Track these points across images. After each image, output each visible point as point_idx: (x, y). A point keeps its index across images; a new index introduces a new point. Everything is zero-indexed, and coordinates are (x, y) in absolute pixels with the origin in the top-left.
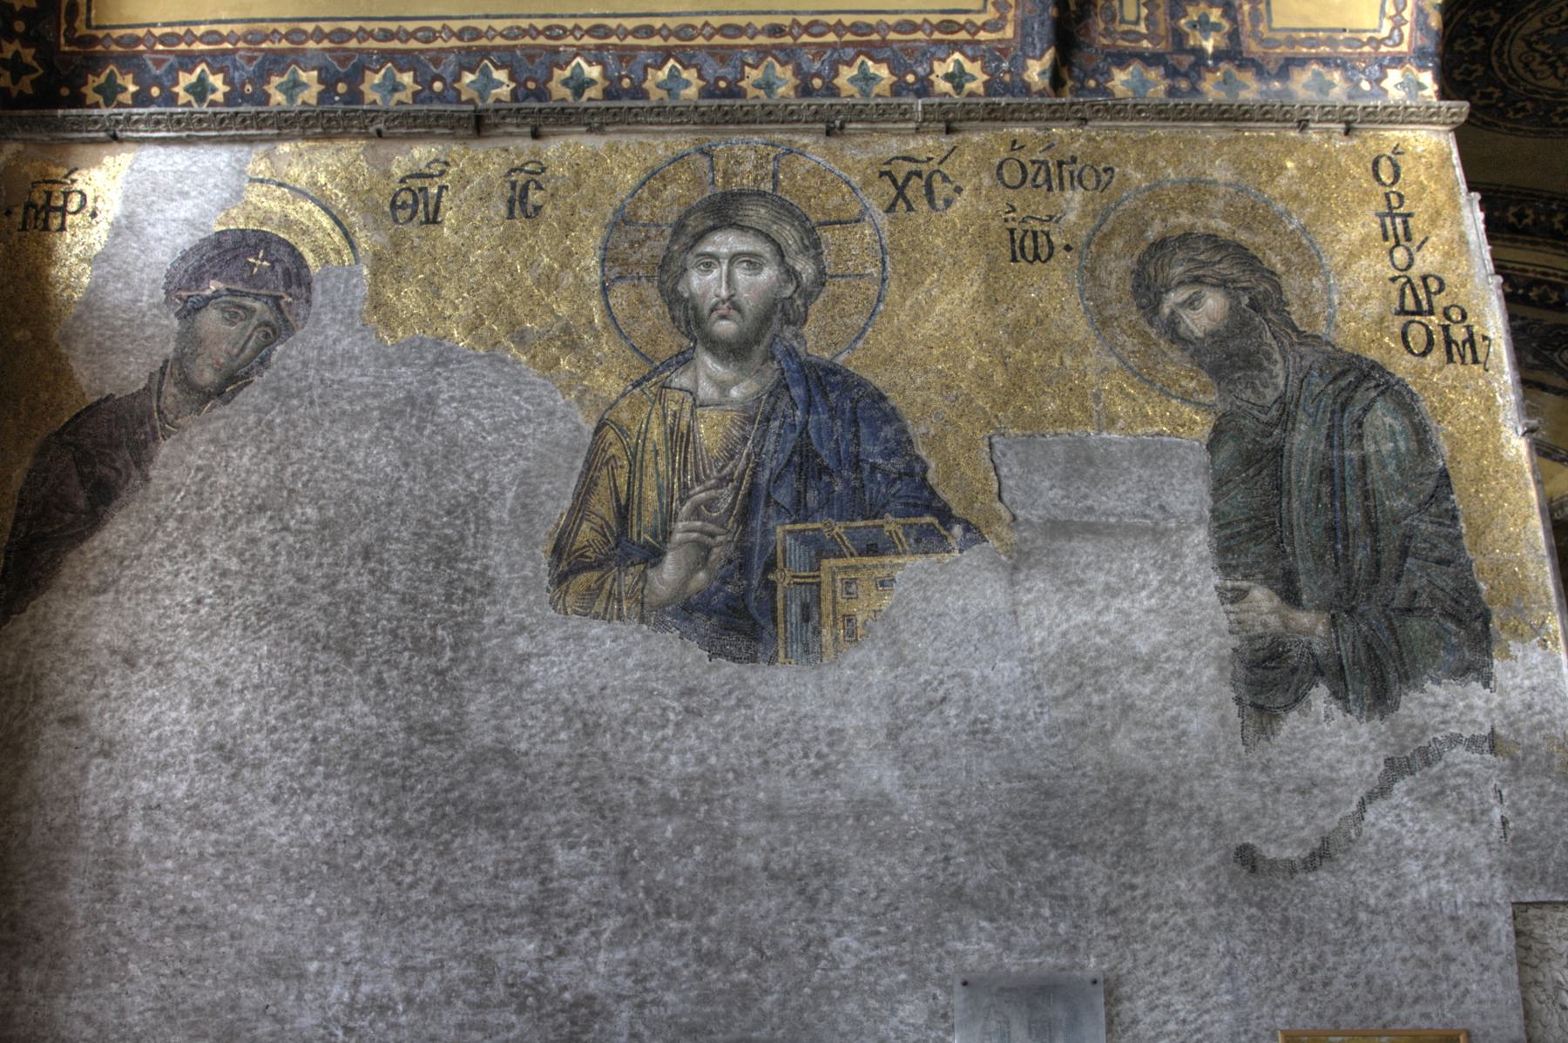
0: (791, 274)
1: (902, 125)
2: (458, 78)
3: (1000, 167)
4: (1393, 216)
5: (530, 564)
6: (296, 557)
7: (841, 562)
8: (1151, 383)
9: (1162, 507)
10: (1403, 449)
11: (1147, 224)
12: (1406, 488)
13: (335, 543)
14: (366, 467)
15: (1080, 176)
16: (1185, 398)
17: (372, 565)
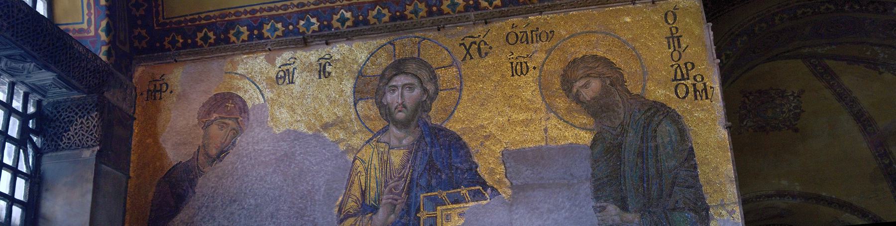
0: (425, 90)
1: (468, 23)
2: (298, 23)
3: (508, 35)
5: (330, 216)
6: (247, 219)
7: (444, 207)
8: (567, 122)
10: (674, 140)
13: (261, 212)
14: (271, 182)
16: (583, 128)
17: (274, 220)
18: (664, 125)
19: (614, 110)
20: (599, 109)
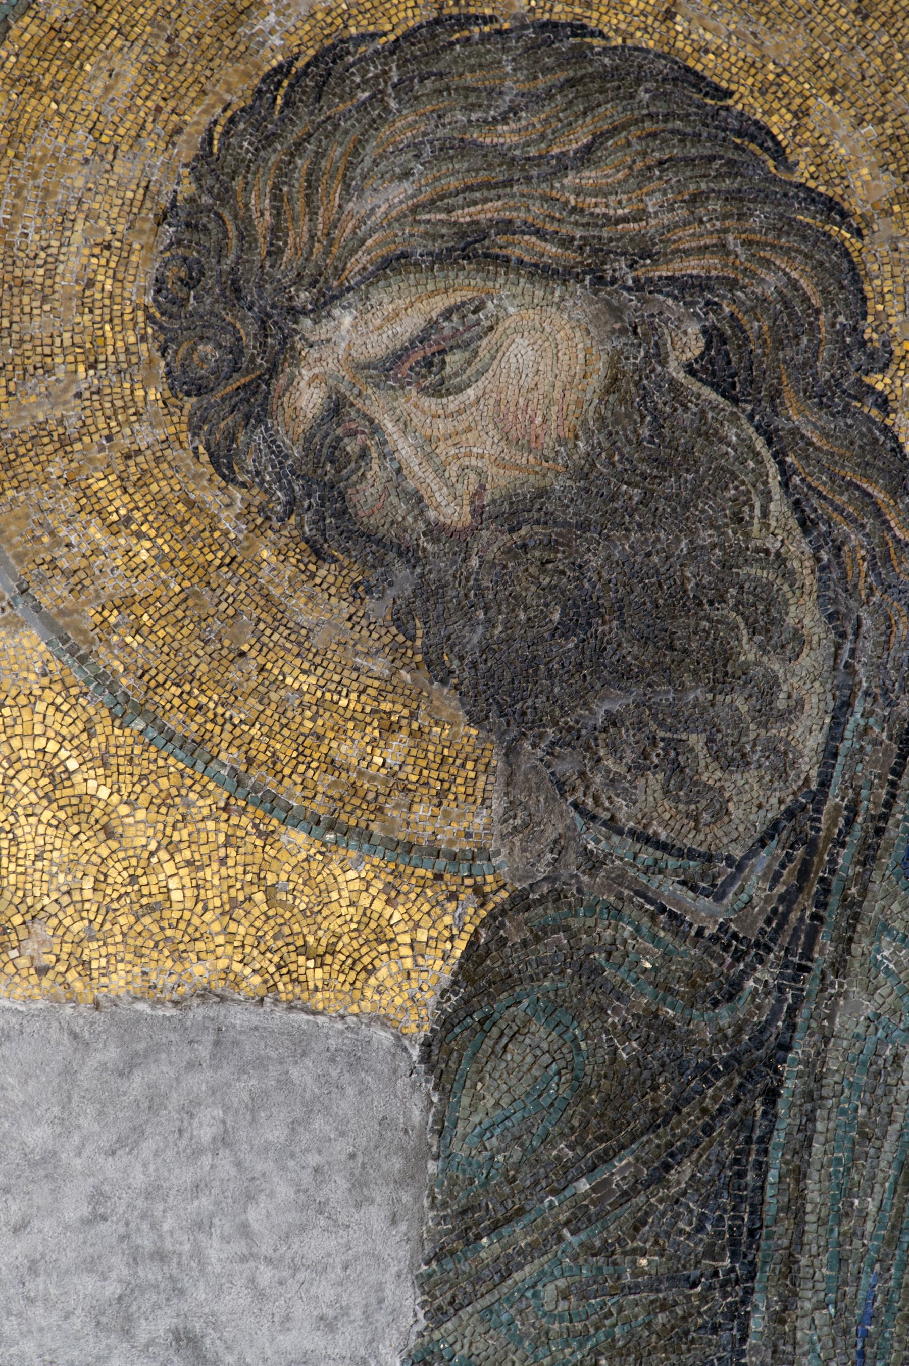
19: (728, 656)
20: (563, 630)
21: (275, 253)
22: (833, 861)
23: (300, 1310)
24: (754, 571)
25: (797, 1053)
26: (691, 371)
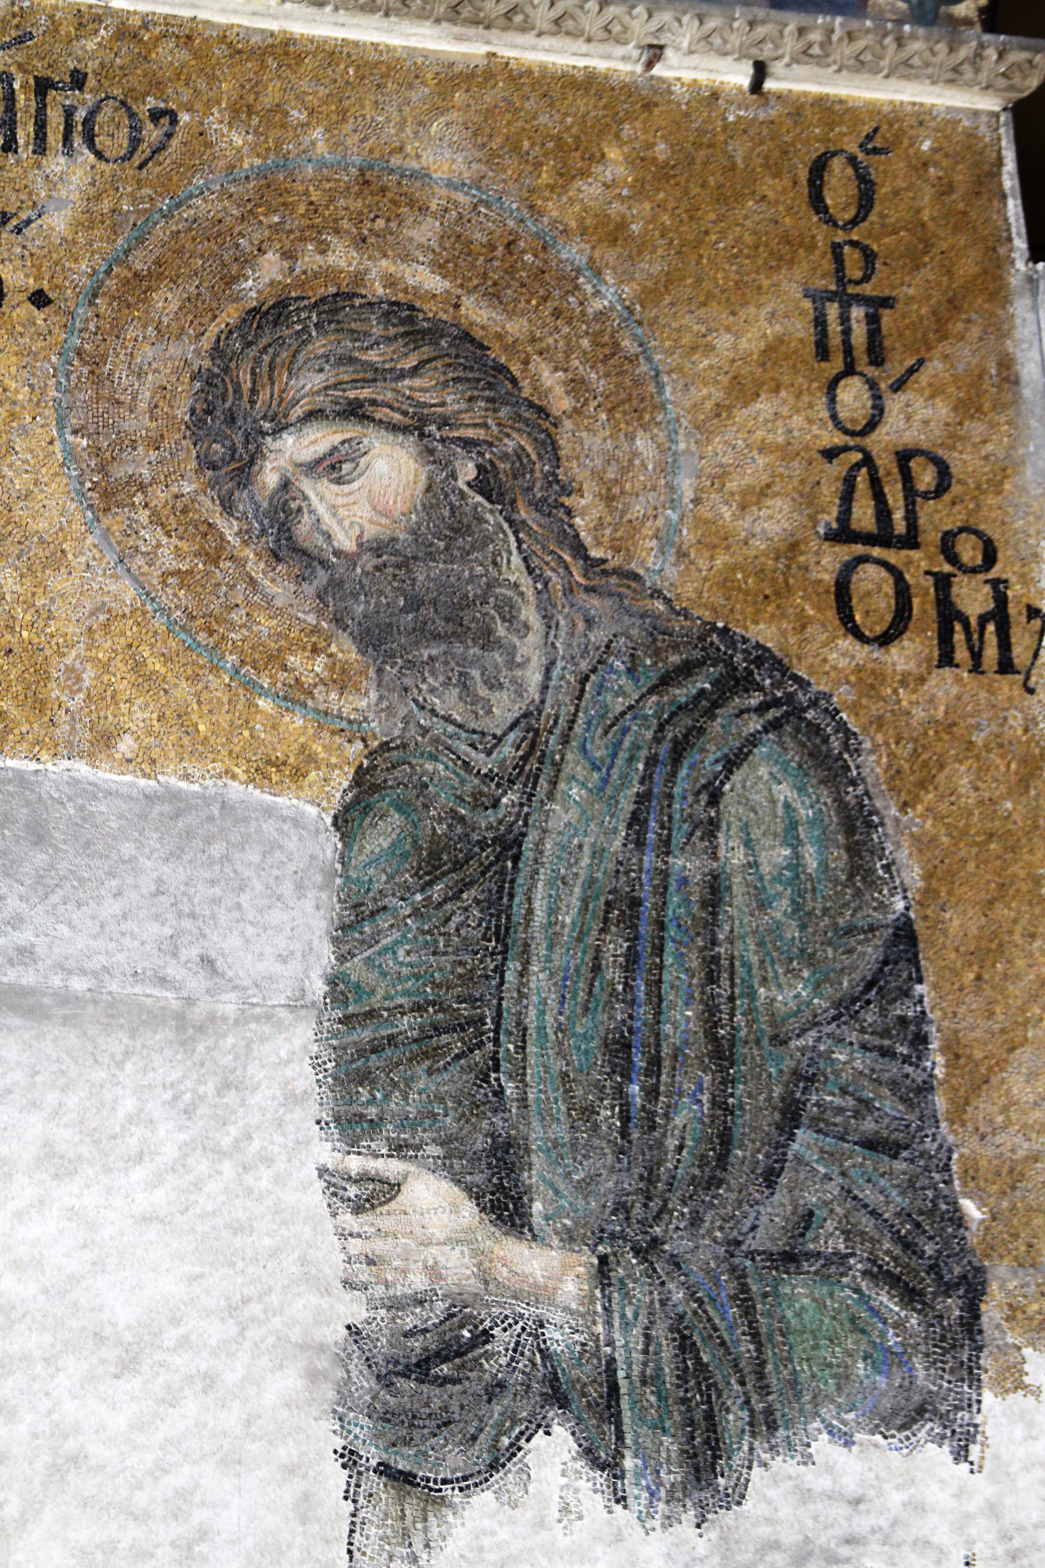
4: (846, 301)
9: (207, 962)
11: (246, 261)
12: (810, 960)
15: (88, 122)
18: (763, 771)
19: (490, 632)
20: (404, 610)
21: (253, 402)
22: (547, 742)
23: (268, 951)
24: (503, 591)
25: (530, 838)
26: (469, 484)
